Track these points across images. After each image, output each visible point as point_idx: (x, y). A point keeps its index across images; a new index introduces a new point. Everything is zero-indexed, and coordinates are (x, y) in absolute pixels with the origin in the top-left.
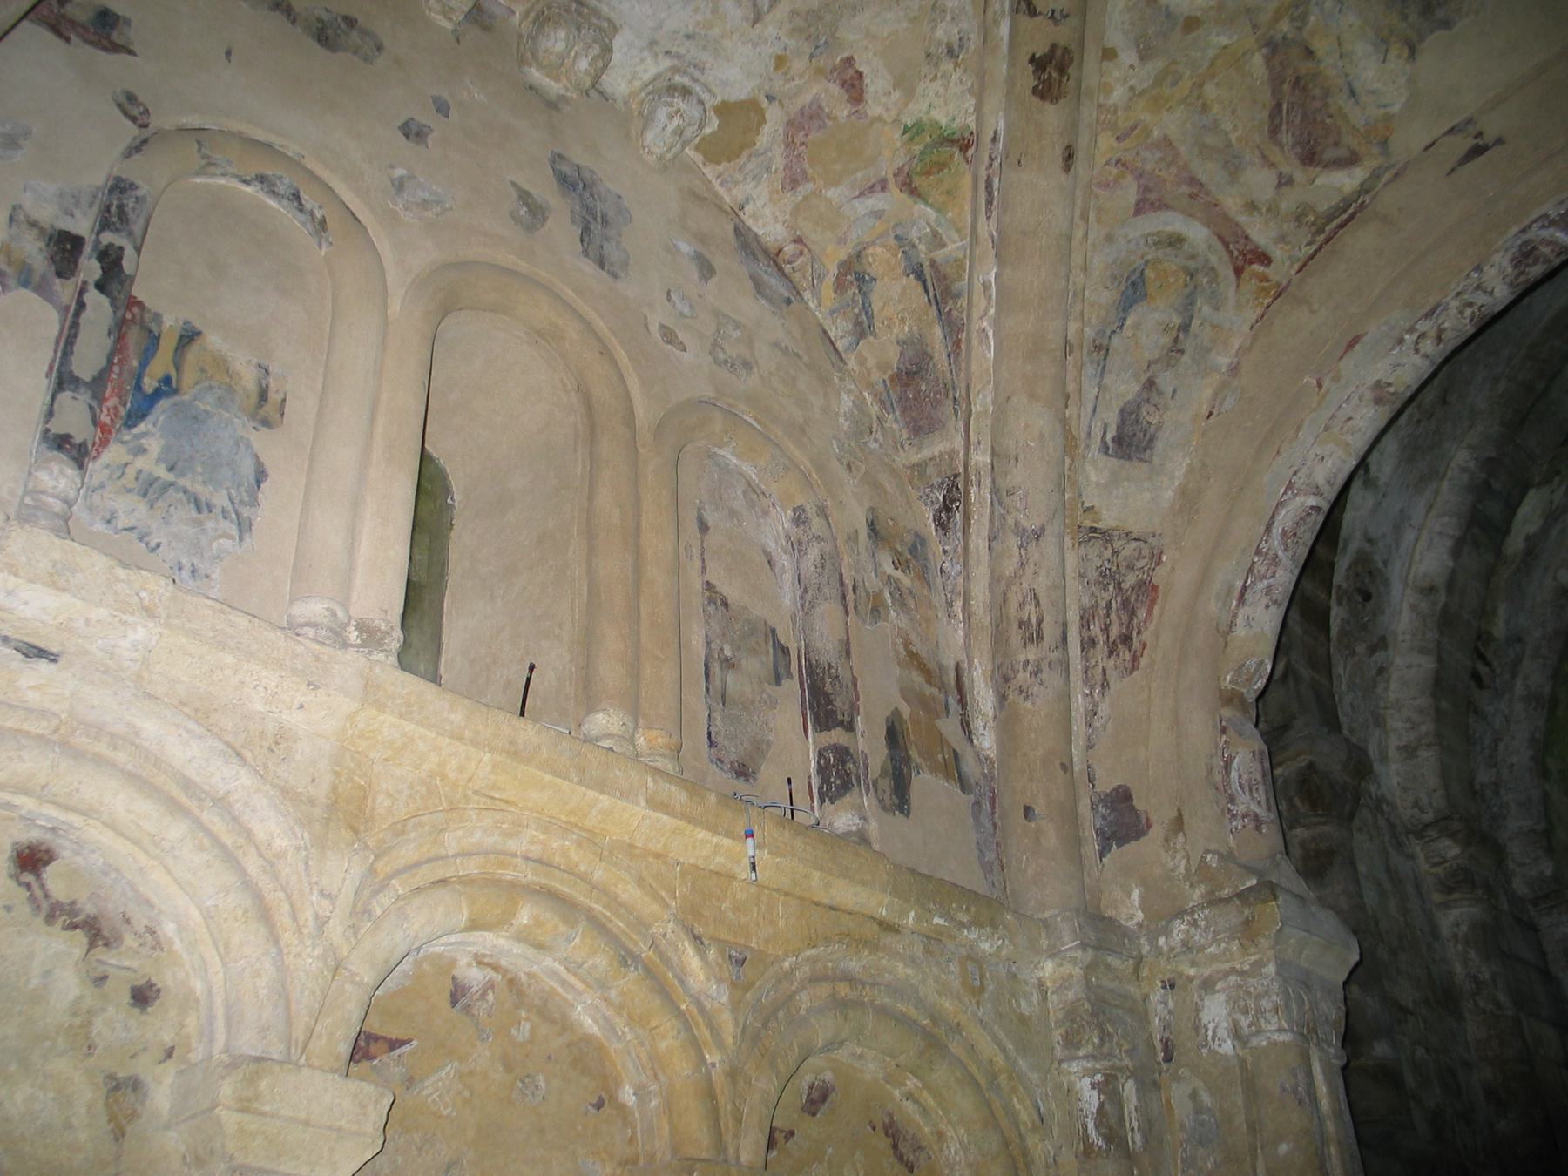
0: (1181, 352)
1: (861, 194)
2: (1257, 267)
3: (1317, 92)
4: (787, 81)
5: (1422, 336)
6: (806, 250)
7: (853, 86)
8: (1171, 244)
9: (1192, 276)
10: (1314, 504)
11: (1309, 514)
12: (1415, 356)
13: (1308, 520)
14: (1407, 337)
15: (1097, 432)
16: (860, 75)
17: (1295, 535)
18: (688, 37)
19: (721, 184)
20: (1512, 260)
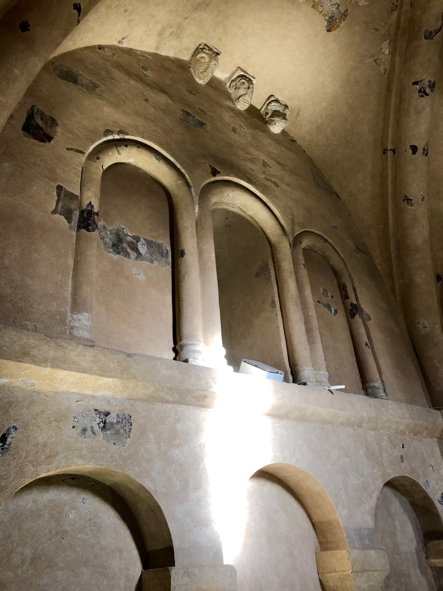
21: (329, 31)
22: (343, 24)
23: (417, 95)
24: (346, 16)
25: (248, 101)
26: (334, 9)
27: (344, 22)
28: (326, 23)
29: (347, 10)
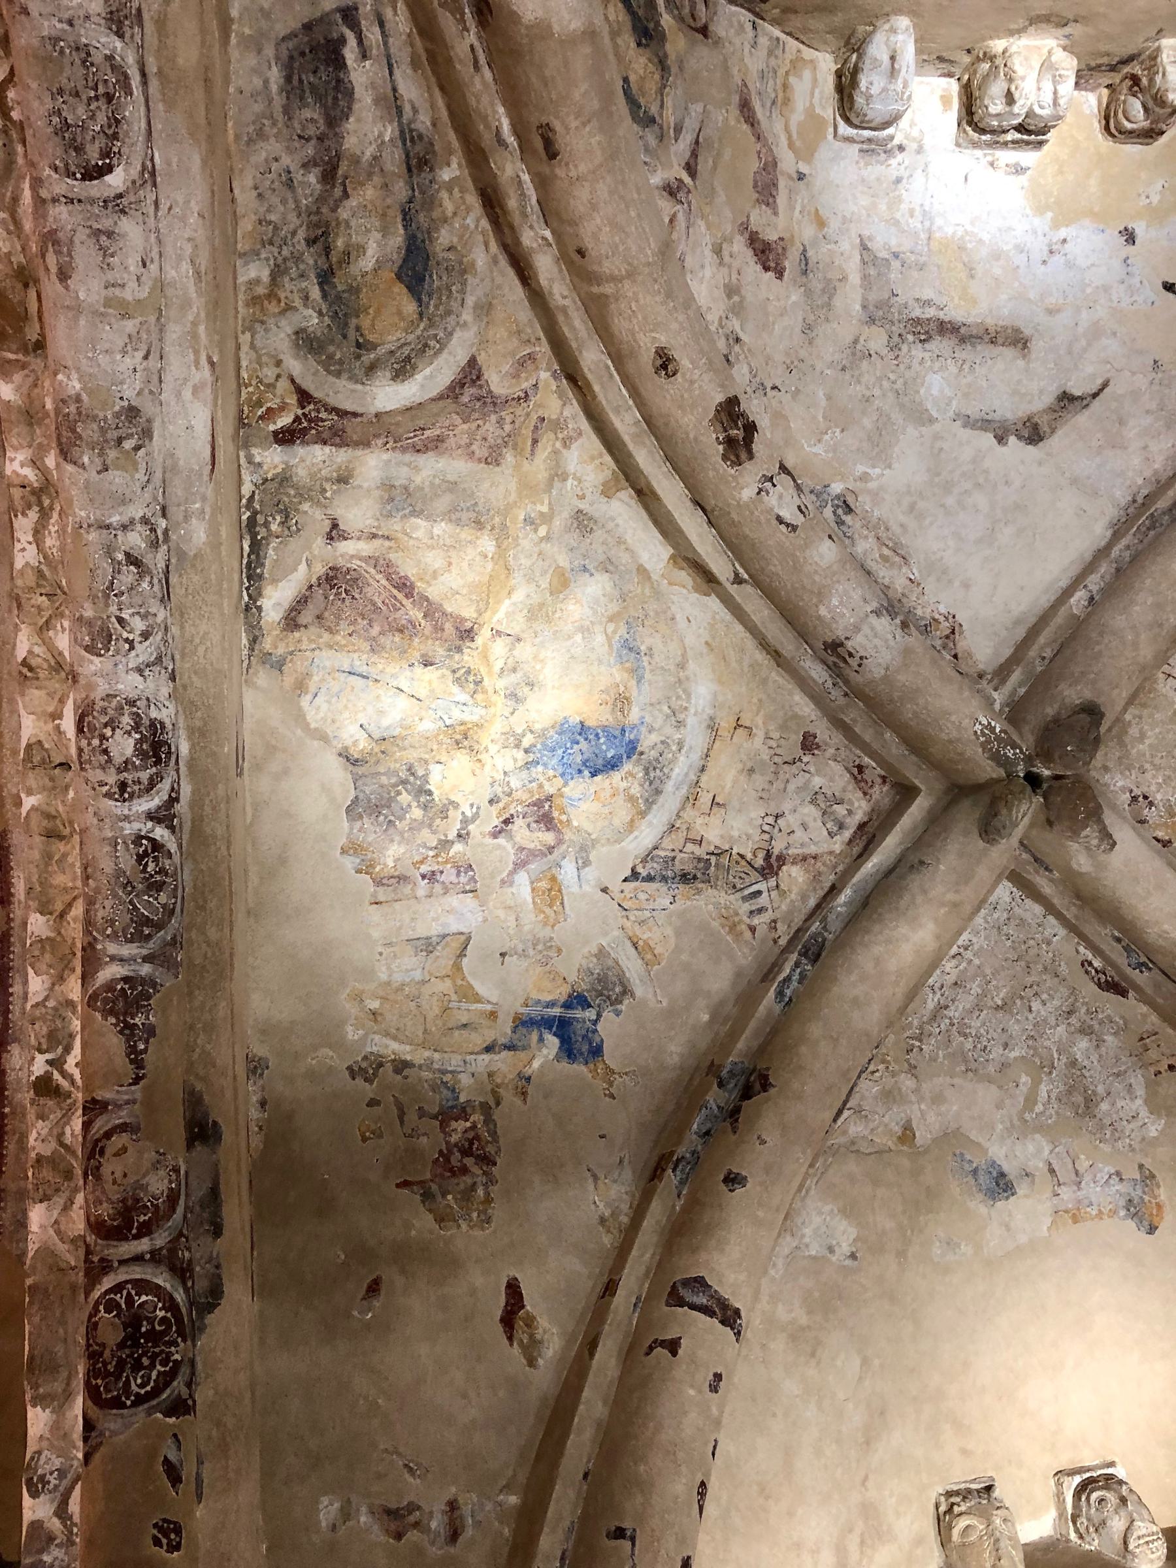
0: (311, 242)
1: (697, 142)
2: (284, 420)
3: (386, 641)
4: (803, 207)
5: (154, 545)
6: (693, 25)
7: (763, 252)
8: (408, 359)
9: (359, 345)
10: (108, 178)
11: (106, 153)
12: (141, 514)
13: (101, 142)
14: (163, 523)
15: (373, 35)
16: (766, 269)
17: (109, 98)
18: (898, 181)
19: (778, 39)
20: (162, 724)
21: (1152, 1230)
22: (1163, 1194)
24: (1153, 1176)
25: (1153, 1534)
26: (1117, 1187)
27: (1162, 1190)
28: (1131, 1224)
29: (1141, 1166)
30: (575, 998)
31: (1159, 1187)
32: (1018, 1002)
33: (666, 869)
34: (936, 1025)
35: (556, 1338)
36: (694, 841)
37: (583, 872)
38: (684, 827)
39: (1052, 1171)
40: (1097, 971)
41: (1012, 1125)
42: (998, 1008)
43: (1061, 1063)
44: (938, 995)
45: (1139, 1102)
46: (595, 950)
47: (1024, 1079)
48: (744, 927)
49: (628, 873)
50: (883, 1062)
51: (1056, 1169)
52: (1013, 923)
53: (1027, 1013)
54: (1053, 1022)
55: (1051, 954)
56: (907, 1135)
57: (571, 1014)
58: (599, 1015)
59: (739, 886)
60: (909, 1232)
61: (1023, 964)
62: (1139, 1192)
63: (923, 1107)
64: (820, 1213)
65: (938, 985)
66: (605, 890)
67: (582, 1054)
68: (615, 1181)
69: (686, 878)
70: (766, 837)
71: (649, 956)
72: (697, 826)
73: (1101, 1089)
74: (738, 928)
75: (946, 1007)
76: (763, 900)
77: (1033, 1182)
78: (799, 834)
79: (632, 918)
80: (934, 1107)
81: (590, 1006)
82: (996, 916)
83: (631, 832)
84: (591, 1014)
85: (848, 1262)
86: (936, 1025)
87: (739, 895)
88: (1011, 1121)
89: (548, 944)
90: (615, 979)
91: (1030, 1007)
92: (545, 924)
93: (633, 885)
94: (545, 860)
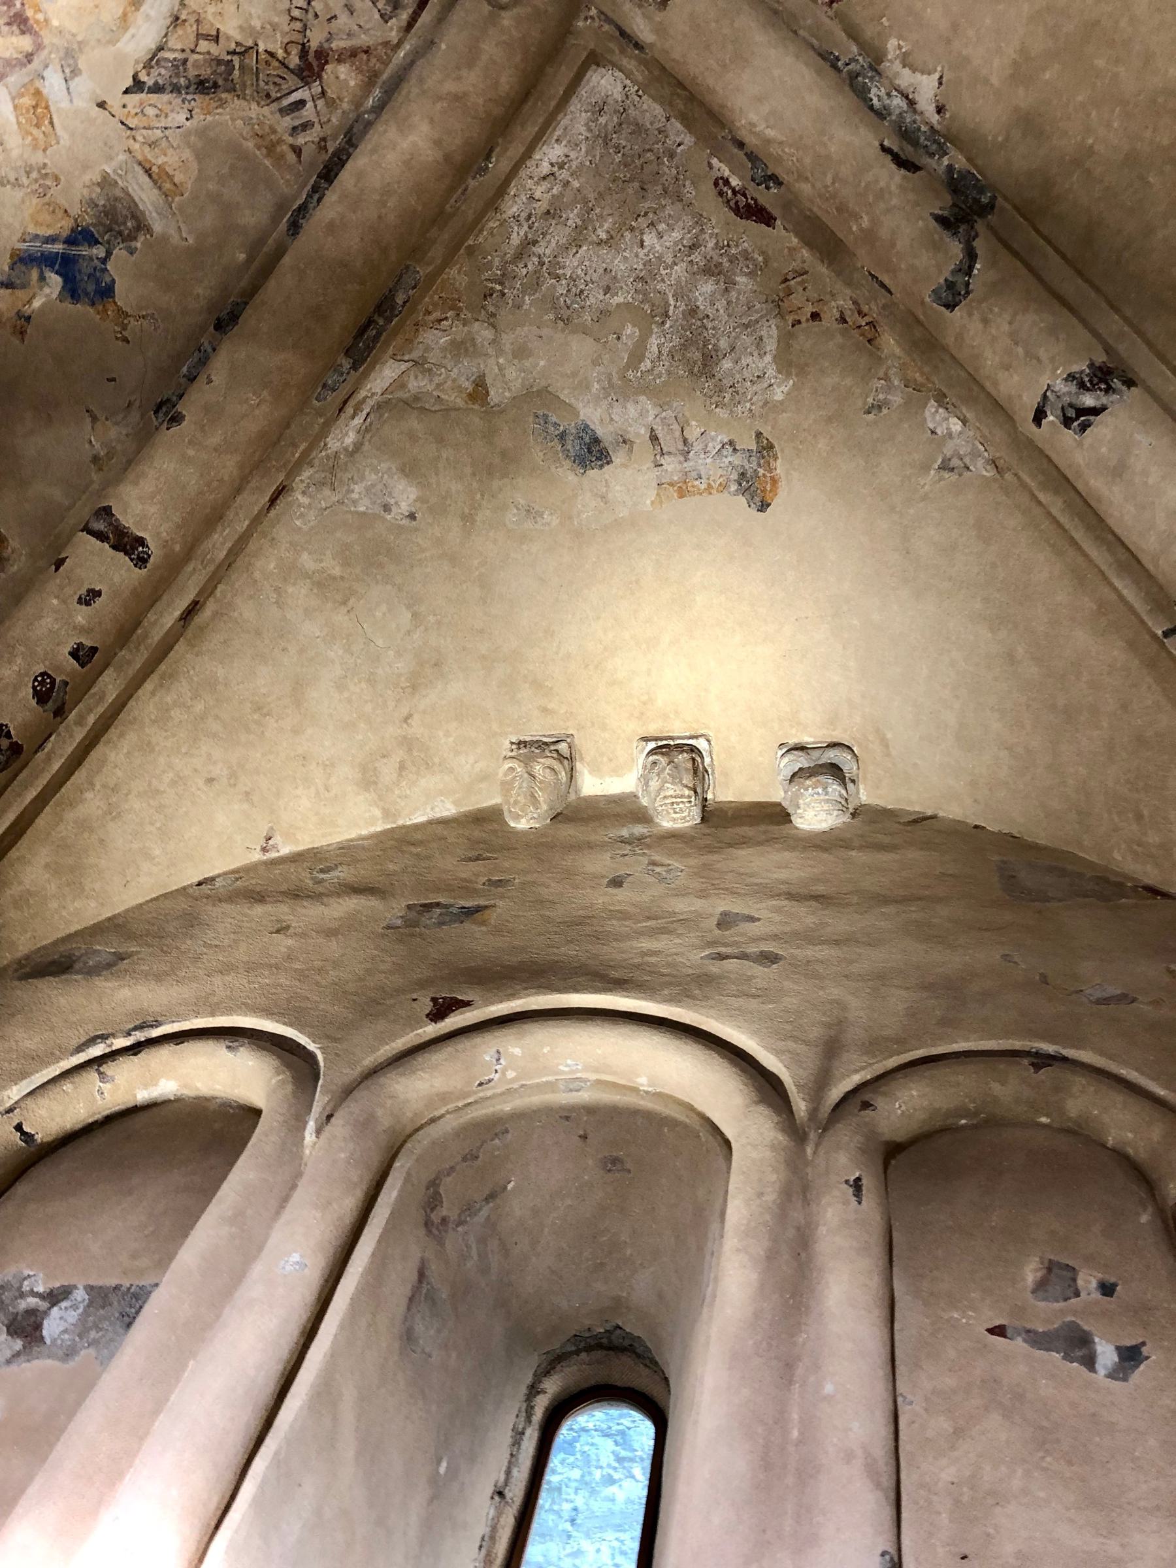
21: (763, 506)
22: (780, 467)
23: (1068, 436)
24: (771, 446)
25: (682, 796)
26: (730, 459)
27: (779, 461)
28: (742, 500)
29: (759, 435)
30: (80, 233)
31: (776, 459)
32: (628, 235)
33: (177, 75)
34: (521, 265)
35: (23, 558)
36: (207, 37)
37: (72, 84)
38: (192, 19)
39: (654, 438)
40: (734, 192)
41: (612, 385)
42: (600, 243)
43: (676, 309)
44: (525, 228)
45: (768, 358)
46: (97, 178)
47: (629, 329)
48: (285, 147)
49: (129, 82)
50: (453, 308)
51: (660, 436)
52: (627, 129)
53: (636, 249)
54: (669, 261)
55: (674, 171)
56: (479, 392)
57: (74, 250)
58: (109, 253)
59: (274, 95)
60: (479, 496)
61: (636, 185)
62: (754, 465)
63: (501, 361)
64: (377, 472)
65: (524, 215)
66: (102, 105)
67: (87, 294)
68: (117, 424)
69: (203, 86)
70: (298, 25)
71: (167, 186)
72: (210, 17)
73: (723, 344)
74: (279, 149)
75: (535, 243)
76: (308, 112)
77: (631, 450)
78: (343, 19)
79: (139, 138)
80: (516, 362)
81: (97, 242)
82: (603, 120)
83: (126, 29)
84: (99, 251)
85: (406, 522)
86: (521, 265)
87: (275, 106)
88: (610, 380)
89: (42, 172)
90: (125, 212)
91: (642, 242)
92: (35, 147)
93: (134, 99)
94: (24, 70)
